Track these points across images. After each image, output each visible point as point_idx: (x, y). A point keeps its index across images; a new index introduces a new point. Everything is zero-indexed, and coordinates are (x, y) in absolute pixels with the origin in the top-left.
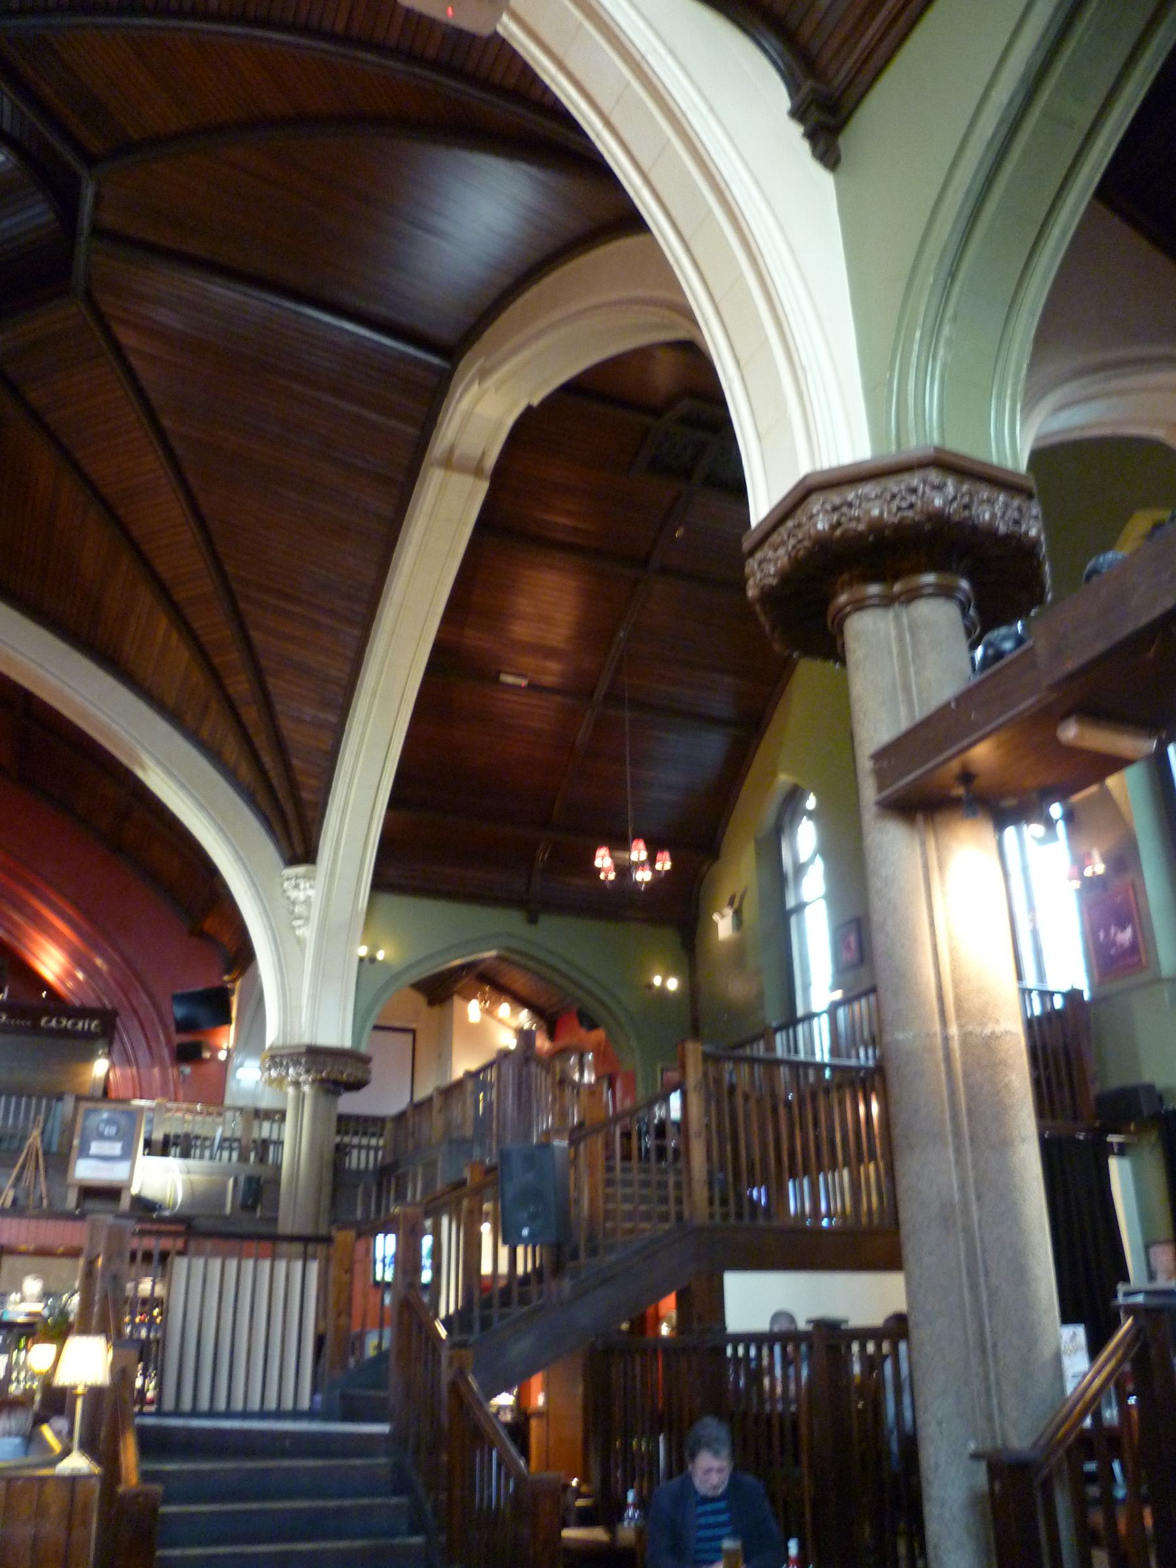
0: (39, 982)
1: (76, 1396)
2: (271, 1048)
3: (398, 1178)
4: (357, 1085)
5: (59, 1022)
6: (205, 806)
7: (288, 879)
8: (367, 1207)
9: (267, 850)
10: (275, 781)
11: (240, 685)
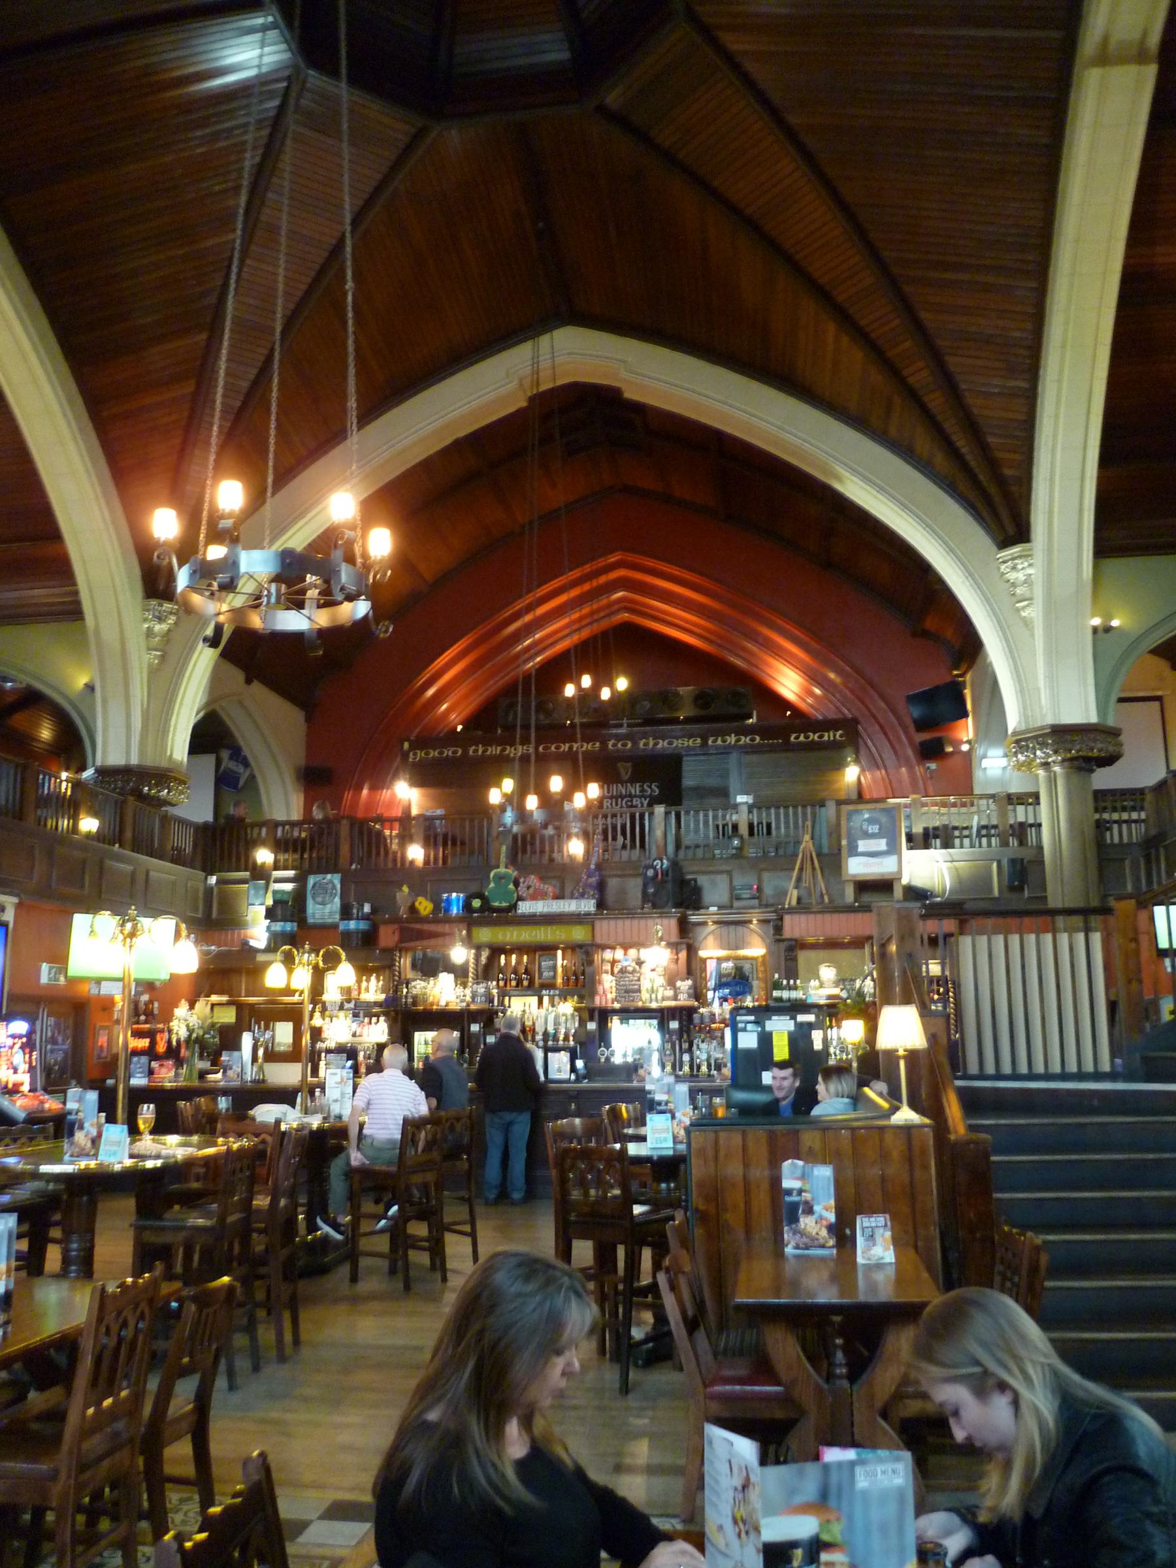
0: (781, 703)
1: (899, 1057)
2: (1015, 733)
3: (1166, 847)
4: (1109, 760)
5: (807, 737)
6: (906, 504)
7: (1004, 562)
8: (1137, 880)
9: (978, 537)
10: (973, 464)
11: (920, 375)
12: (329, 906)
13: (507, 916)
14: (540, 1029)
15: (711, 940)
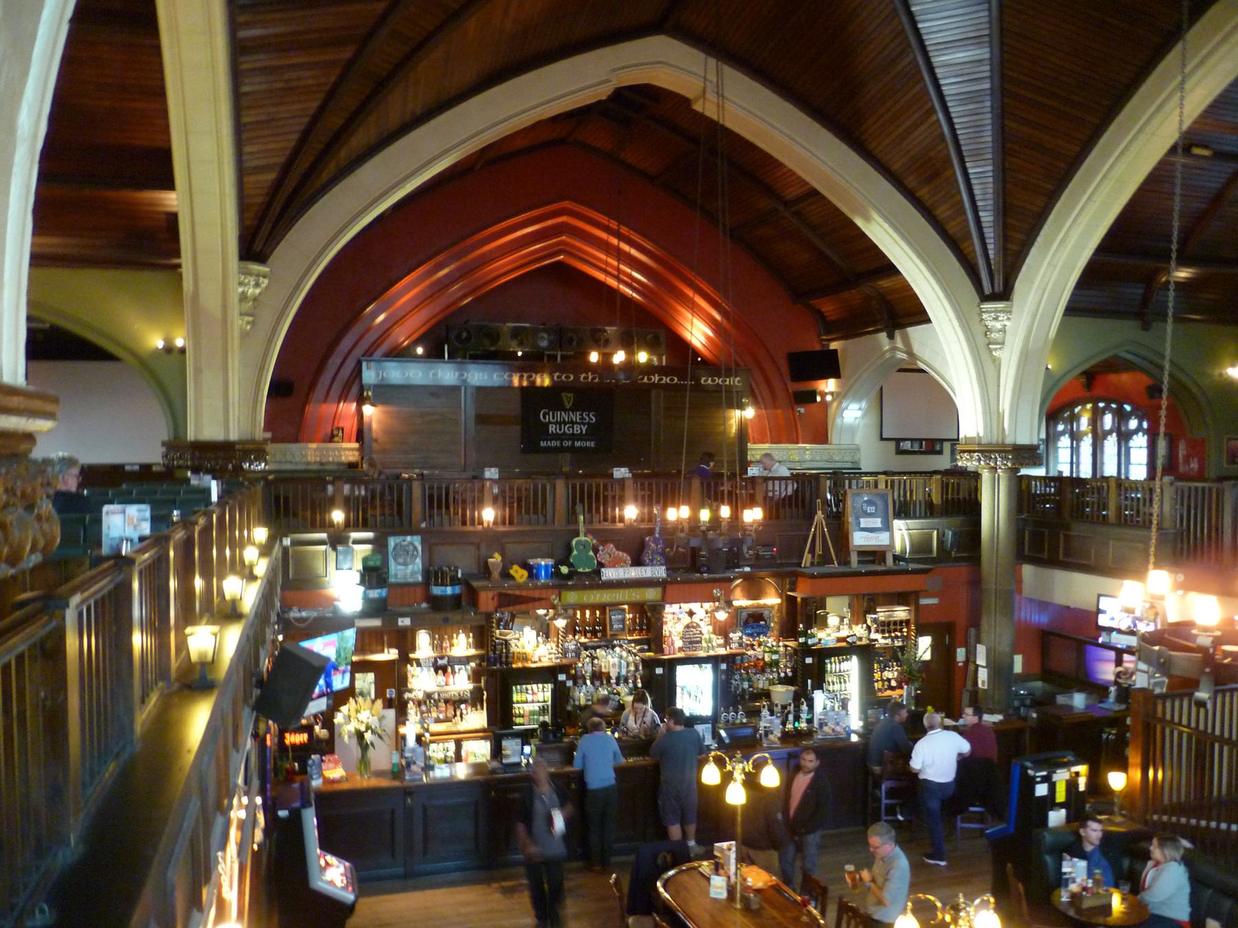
5: (713, 381)
12: (410, 567)
13: (593, 580)
14: (613, 675)
15: (738, 593)
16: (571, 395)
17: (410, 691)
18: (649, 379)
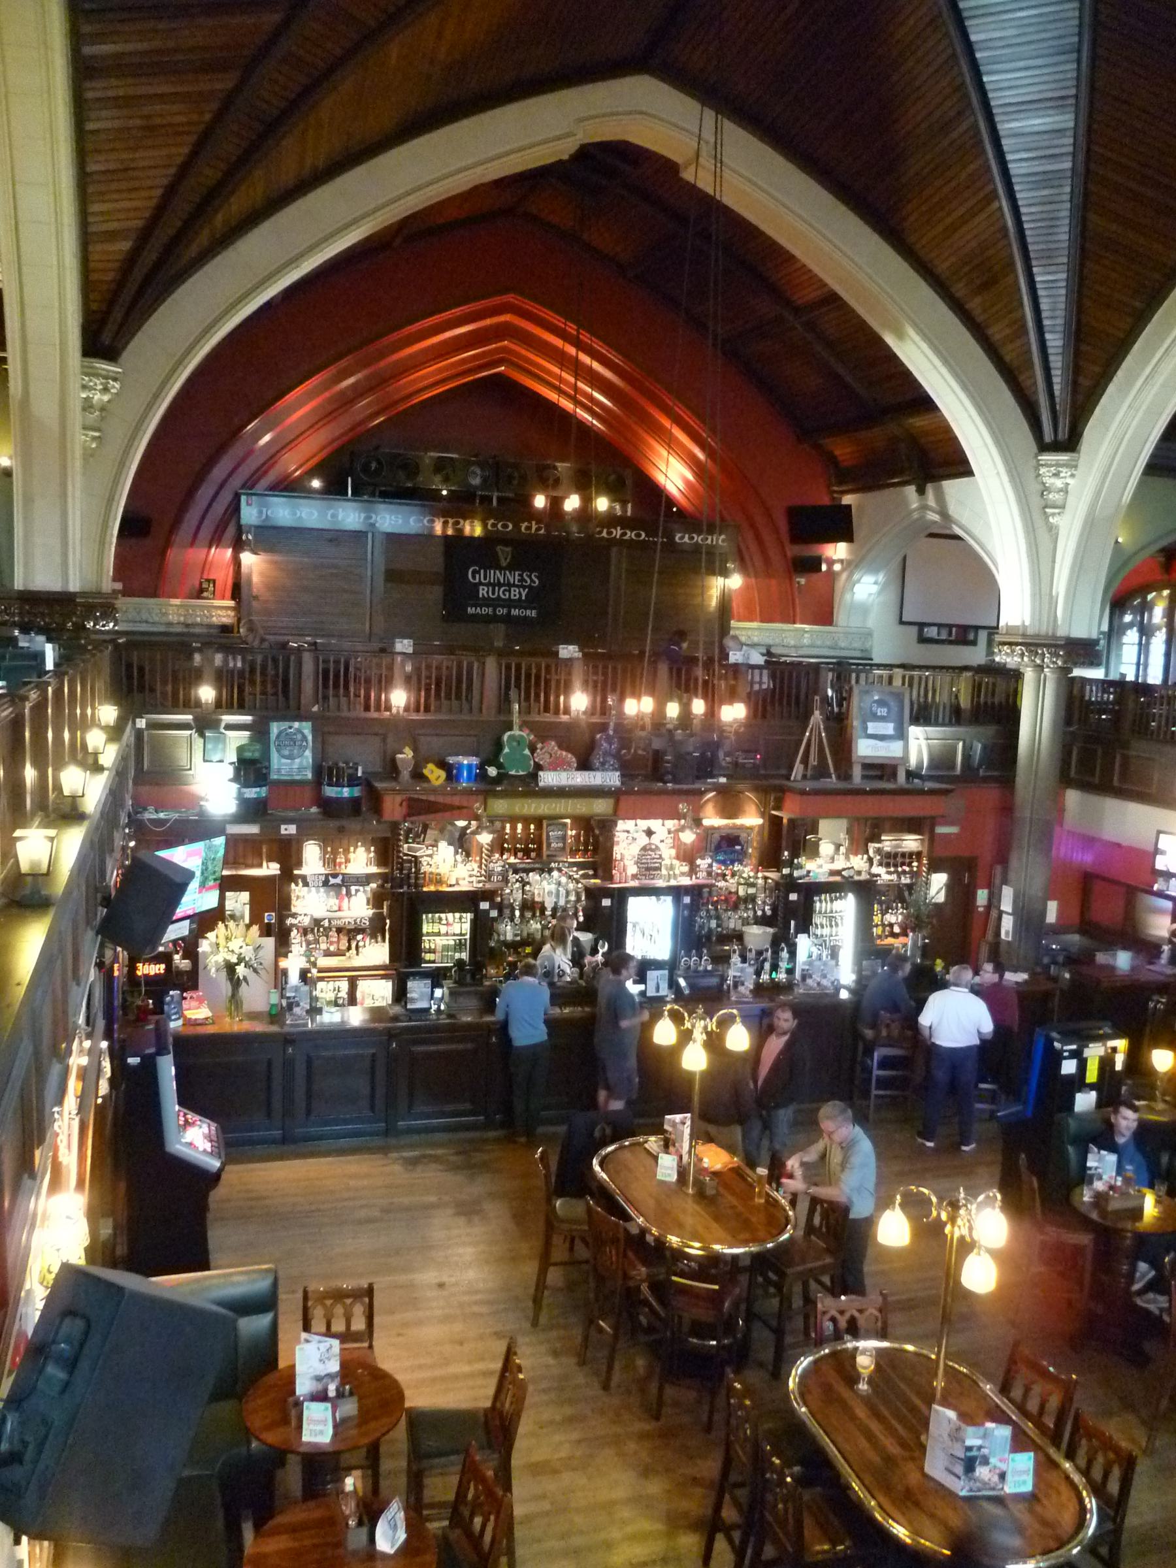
12: (297, 761)
13: (528, 786)
14: (549, 905)
15: (709, 809)
16: (509, 549)
17: (294, 916)
18: (609, 533)
